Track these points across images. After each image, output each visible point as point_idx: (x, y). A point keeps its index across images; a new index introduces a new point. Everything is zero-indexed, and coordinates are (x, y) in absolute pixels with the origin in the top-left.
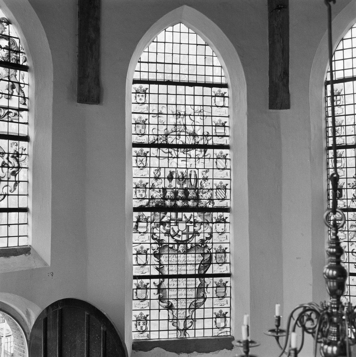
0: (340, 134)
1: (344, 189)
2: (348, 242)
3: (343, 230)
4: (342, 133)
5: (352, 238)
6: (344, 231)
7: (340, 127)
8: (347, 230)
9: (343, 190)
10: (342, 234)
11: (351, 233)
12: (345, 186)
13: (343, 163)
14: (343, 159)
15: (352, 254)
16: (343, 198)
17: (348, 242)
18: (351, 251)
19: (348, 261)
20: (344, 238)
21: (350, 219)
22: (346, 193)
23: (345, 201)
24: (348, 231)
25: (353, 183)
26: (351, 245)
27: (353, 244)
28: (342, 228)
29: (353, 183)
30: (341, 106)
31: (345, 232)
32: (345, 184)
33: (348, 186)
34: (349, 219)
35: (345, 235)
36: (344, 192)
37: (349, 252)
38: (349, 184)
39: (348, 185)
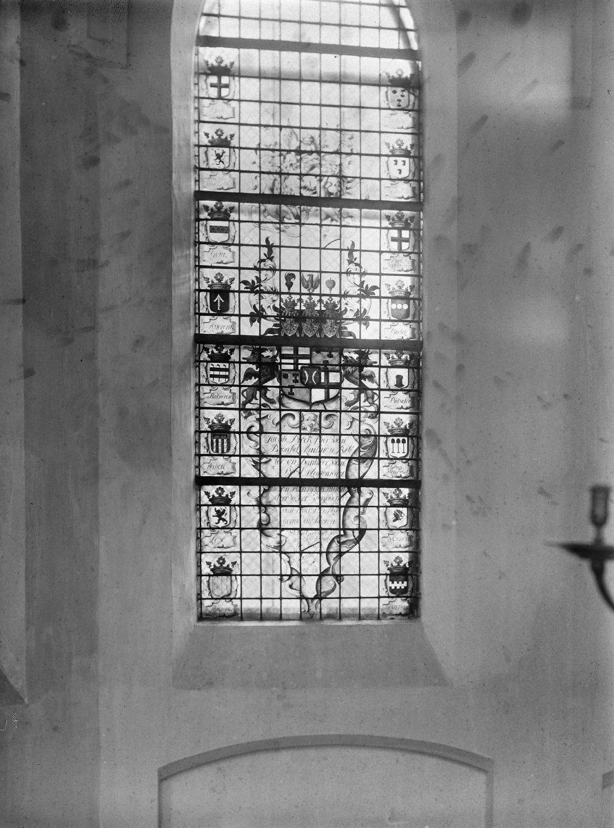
0: (227, 165)
1: (234, 292)
2: (239, 409)
3: (229, 383)
4: (232, 164)
5: (249, 401)
6: (231, 386)
7: (228, 149)
8: (237, 383)
9: (231, 294)
10: (227, 393)
11: (245, 390)
12: (234, 286)
13: (232, 233)
14: (231, 223)
15: (250, 438)
16: (229, 313)
17: (239, 409)
18: (245, 430)
19: (237, 453)
20: (231, 400)
21: (244, 359)
22: (238, 303)
23: (235, 319)
24: (240, 386)
25: (253, 281)
26: (246, 418)
27: (250, 414)
28: (227, 379)
29: (253, 281)
30: (230, 100)
31: (232, 388)
32: (236, 281)
33: (243, 287)
34: (242, 360)
35: (234, 394)
36: (233, 299)
37: (240, 433)
38: (245, 282)
39: (242, 285)
